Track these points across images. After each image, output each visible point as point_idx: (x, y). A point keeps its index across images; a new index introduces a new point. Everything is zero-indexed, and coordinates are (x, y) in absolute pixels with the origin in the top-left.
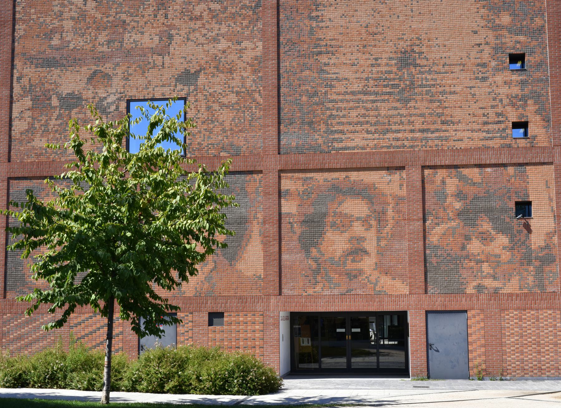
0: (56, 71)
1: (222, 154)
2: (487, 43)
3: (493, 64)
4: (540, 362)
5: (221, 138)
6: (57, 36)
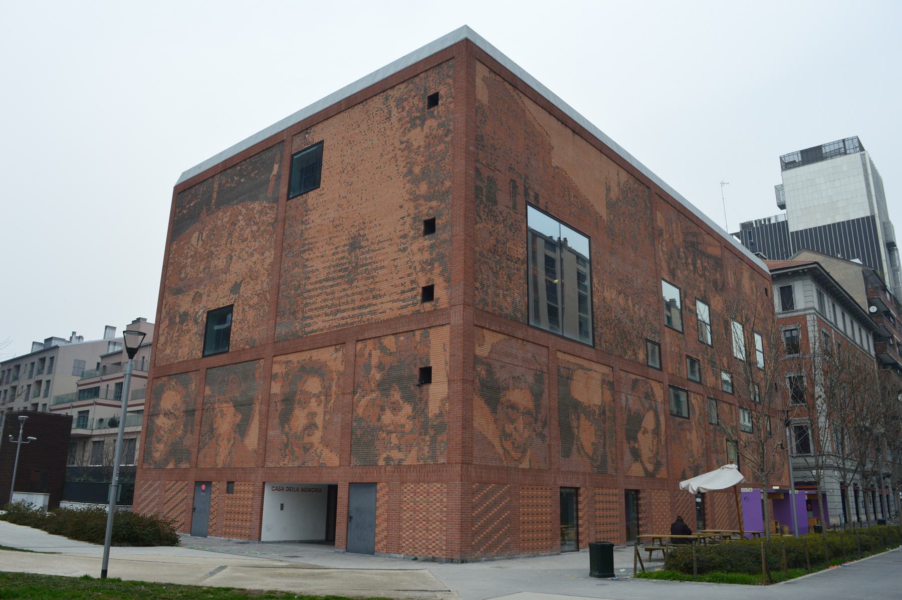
0: (181, 297)
1: (247, 347)
2: (409, 215)
3: (412, 233)
4: (427, 540)
5: (246, 334)
6: (184, 270)
